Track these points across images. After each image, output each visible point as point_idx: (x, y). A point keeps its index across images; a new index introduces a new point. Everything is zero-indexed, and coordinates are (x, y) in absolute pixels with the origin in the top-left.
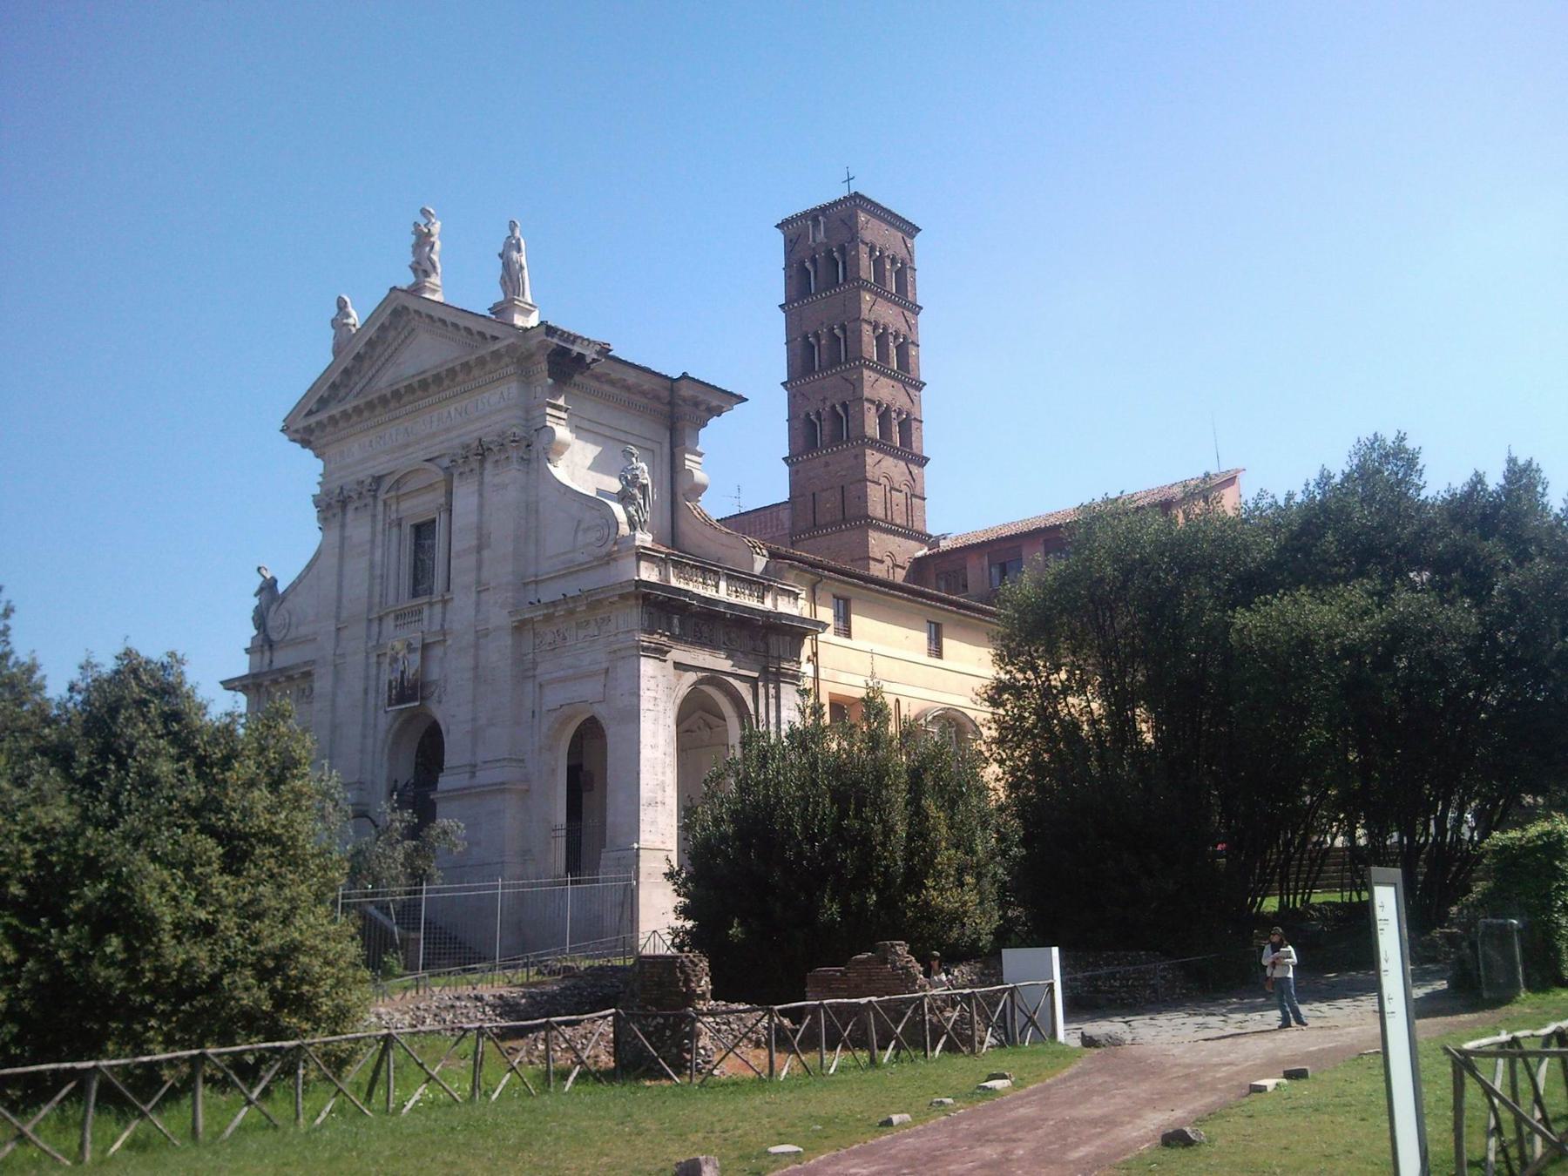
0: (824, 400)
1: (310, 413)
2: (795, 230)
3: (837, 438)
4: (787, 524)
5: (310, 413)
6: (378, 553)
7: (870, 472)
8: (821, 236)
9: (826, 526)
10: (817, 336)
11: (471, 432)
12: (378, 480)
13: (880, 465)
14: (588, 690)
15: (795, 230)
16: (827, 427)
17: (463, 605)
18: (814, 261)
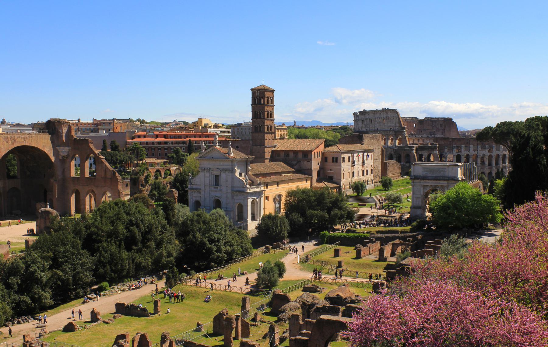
0: (258, 124)
1: (199, 158)
2: (255, 92)
3: (260, 131)
4: (251, 144)
5: (199, 158)
6: (210, 178)
7: (266, 138)
8: (258, 94)
9: (258, 146)
10: (257, 112)
11: (225, 167)
12: (210, 168)
13: (267, 137)
14: (241, 202)
15: (255, 92)
16: (258, 129)
17: (224, 188)
18: (257, 98)
